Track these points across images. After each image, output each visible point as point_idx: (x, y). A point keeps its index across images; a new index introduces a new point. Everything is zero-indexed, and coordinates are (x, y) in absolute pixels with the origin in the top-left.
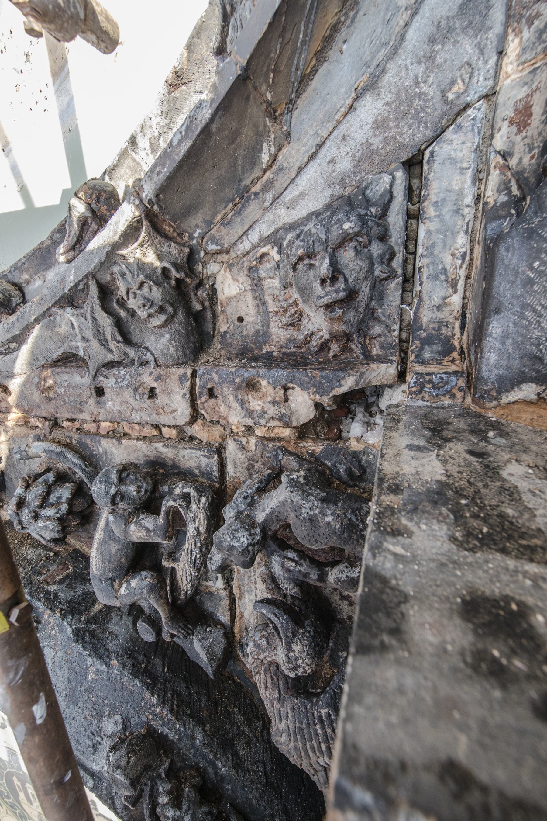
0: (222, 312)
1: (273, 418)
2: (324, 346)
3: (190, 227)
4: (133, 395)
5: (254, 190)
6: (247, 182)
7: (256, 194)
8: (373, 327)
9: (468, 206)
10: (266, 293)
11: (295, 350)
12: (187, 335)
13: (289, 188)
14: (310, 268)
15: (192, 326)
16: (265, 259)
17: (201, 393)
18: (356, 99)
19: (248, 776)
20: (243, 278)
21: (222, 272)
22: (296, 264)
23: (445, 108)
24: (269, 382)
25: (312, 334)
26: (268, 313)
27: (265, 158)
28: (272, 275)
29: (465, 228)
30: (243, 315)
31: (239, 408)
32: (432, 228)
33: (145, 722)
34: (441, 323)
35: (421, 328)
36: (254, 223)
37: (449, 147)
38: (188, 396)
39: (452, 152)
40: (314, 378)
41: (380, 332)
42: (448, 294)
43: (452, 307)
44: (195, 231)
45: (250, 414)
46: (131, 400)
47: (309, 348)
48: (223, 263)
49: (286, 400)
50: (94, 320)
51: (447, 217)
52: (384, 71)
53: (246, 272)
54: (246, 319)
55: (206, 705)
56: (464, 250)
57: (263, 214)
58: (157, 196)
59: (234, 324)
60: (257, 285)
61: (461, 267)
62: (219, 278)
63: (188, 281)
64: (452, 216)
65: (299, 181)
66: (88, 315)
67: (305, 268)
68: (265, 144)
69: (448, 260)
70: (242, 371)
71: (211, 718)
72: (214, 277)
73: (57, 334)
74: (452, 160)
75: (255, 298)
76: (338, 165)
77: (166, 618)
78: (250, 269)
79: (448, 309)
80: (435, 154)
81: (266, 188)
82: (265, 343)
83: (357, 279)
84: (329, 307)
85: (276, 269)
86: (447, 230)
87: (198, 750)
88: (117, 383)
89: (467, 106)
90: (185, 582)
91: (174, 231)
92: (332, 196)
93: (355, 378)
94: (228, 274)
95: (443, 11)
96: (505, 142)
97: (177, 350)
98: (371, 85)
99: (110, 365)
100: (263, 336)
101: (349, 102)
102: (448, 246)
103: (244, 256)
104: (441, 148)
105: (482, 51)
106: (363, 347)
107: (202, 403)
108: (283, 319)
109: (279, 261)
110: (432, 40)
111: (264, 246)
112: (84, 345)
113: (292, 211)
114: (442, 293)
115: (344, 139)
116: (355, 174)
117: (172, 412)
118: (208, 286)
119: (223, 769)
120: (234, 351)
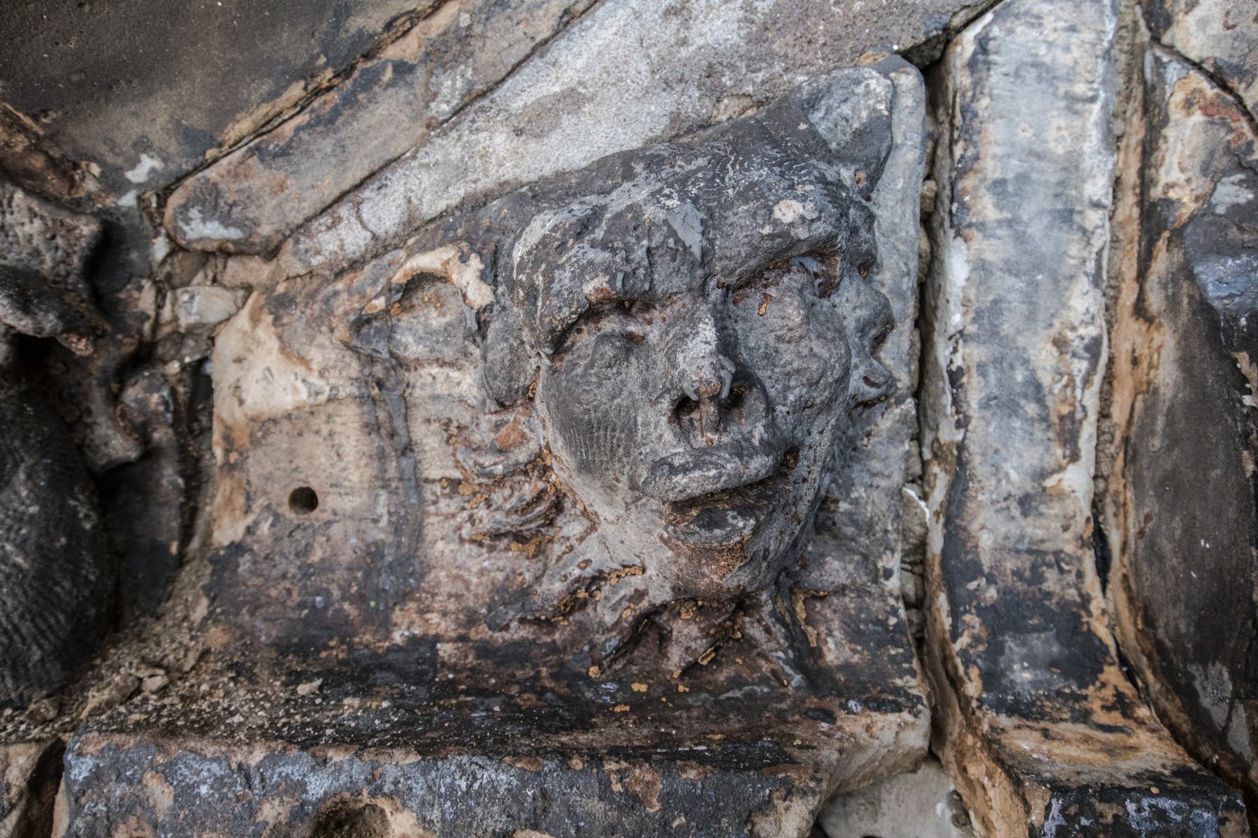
0: (229, 467)
2: (648, 628)
3: (113, 147)
5: (393, 52)
7: (403, 69)
8: (820, 560)
9: (1097, 205)
10: (418, 415)
11: (525, 633)
12: (43, 576)
13: (526, 70)
14: (629, 351)
15: (73, 530)
16: (427, 293)
20: (324, 351)
21: (243, 320)
22: (570, 328)
24: (425, 823)
25: (599, 578)
26: (419, 483)
28: (449, 353)
29: (1091, 266)
30: (314, 485)
32: (989, 256)
34: (1041, 558)
35: (975, 570)
36: (387, 165)
37: (1034, 33)
39: (1042, 50)
40: (634, 801)
41: (842, 578)
42: (1050, 462)
43: (1070, 507)
44: (134, 163)
47: (582, 628)
48: (249, 289)
51: (1035, 230)
53: (342, 332)
54: (329, 502)
56: (1092, 331)
57: (425, 141)
59: (277, 517)
60: (383, 388)
61: (1087, 382)
62: (228, 344)
63: (81, 347)
64: (1050, 227)
65: (561, 50)
67: (609, 351)
69: (1044, 357)
70: (295, 766)
74: (1046, 73)
75: (372, 427)
76: (697, 27)
78: (361, 323)
79: (1055, 509)
80: (991, 45)
81: (441, 55)
82: (404, 597)
83: (803, 406)
84: (700, 509)
85: (470, 336)
86: (1037, 268)
91: (36, 146)
92: (675, 118)
93: (813, 802)
94: (265, 333)
96: (1218, 39)
100: (394, 569)
102: (1042, 316)
103: (339, 274)
104: (1010, 32)
106: (789, 637)
108: (482, 512)
109: (488, 308)
111: (424, 248)
113: (533, 145)
114: (1032, 457)
116: (753, 63)
118: (174, 367)
120: (266, 633)
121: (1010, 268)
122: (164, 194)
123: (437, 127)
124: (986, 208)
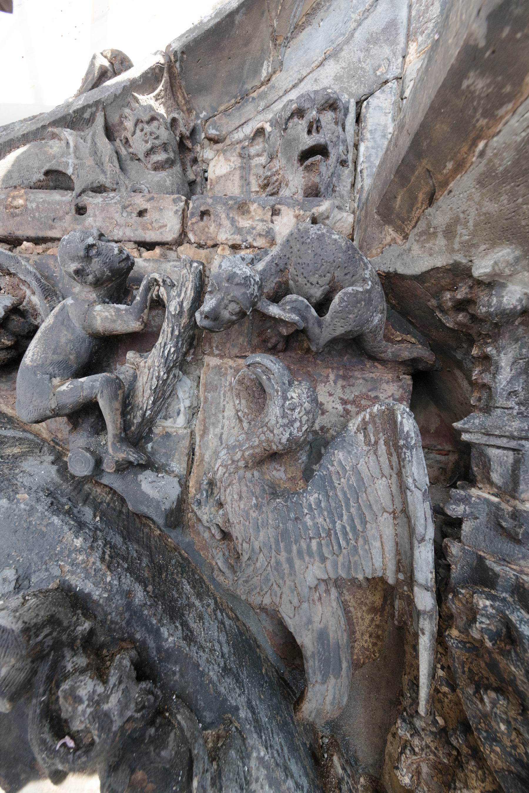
1: (260, 235)
4: (119, 210)
5: (252, 95)
6: (248, 86)
7: (253, 99)
17: (193, 214)
18: (325, 59)
19: (201, 653)
23: (376, 79)
27: (264, 73)
31: (229, 225)
33: (57, 577)
38: (180, 213)
44: (202, 113)
45: (239, 231)
46: (117, 216)
49: (272, 222)
50: (94, 143)
51: (378, 139)
52: (341, 50)
55: (147, 565)
57: (256, 115)
58: (183, 53)
62: (212, 164)
66: (89, 138)
68: (265, 62)
71: (154, 581)
72: (207, 162)
73: (46, 153)
74: (380, 108)
75: (242, 177)
77: (115, 436)
81: (262, 96)
86: (378, 147)
87: (135, 613)
88: (104, 200)
89: (386, 82)
90: (146, 395)
94: (222, 158)
95: (374, 29)
97: (173, 184)
98: (333, 54)
99: (99, 189)
101: (320, 59)
105: (394, 54)
107: (192, 224)
110: (368, 41)
112: (76, 162)
115: (316, 80)
117: (161, 227)
119: (171, 639)
121: (373, 148)
122: (206, 121)
123: (259, 112)
124: (368, 135)
